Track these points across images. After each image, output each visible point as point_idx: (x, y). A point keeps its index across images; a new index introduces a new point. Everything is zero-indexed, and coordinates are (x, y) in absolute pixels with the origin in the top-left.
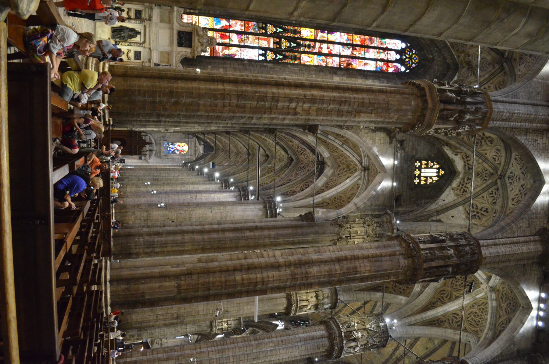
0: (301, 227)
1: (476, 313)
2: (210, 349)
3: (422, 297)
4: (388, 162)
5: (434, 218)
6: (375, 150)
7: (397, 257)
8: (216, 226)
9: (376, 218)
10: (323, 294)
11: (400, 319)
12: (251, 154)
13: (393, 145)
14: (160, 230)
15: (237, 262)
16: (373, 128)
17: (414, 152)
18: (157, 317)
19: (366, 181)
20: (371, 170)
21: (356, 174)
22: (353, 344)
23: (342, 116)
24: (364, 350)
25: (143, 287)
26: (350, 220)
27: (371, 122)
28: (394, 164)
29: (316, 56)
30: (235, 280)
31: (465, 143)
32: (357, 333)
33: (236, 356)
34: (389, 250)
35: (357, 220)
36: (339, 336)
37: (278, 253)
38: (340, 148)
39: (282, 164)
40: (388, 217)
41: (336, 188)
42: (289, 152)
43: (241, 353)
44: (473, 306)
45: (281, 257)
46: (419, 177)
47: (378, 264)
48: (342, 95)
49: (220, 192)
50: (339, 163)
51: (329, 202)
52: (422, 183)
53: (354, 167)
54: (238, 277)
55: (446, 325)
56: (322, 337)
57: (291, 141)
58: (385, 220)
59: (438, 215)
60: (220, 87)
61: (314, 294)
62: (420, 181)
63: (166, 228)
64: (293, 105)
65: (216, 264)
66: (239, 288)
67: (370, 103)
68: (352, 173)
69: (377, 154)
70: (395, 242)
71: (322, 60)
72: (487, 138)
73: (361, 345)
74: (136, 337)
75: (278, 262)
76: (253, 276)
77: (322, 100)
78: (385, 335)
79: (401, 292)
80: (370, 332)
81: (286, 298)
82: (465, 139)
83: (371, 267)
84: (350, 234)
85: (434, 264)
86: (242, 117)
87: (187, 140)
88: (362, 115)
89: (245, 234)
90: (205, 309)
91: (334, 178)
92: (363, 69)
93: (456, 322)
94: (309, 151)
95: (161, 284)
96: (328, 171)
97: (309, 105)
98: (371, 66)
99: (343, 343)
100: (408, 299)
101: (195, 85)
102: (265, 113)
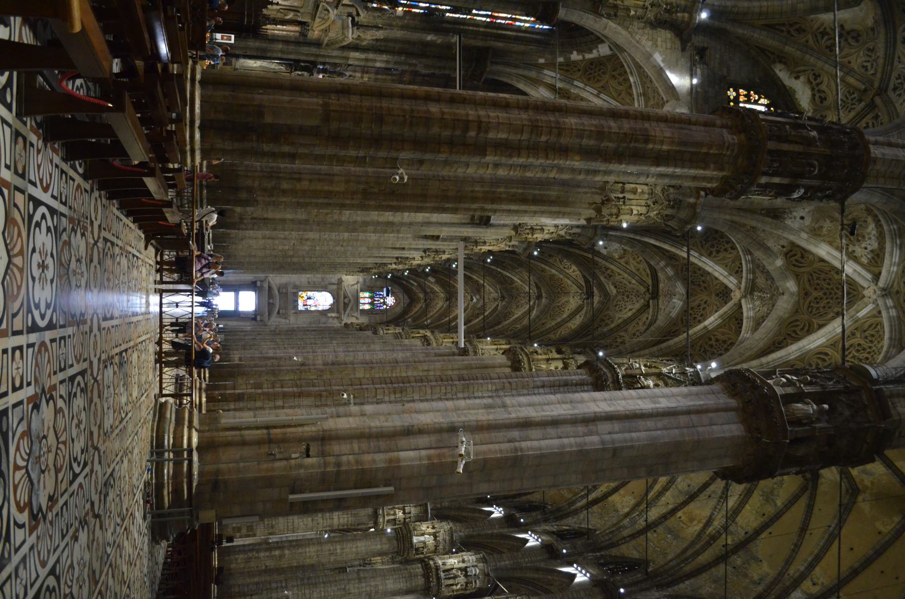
1: (859, 345)
4: (679, 80)
6: (658, 58)
17: (725, 70)
28: (692, 85)
31: (812, 49)
36: (613, 382)
44: (853, 334)
66: (435, 130)
69: (662, 65)
72: (848, 33)
74: (244, 531)
81: (511, 367)
82: (811, 42)
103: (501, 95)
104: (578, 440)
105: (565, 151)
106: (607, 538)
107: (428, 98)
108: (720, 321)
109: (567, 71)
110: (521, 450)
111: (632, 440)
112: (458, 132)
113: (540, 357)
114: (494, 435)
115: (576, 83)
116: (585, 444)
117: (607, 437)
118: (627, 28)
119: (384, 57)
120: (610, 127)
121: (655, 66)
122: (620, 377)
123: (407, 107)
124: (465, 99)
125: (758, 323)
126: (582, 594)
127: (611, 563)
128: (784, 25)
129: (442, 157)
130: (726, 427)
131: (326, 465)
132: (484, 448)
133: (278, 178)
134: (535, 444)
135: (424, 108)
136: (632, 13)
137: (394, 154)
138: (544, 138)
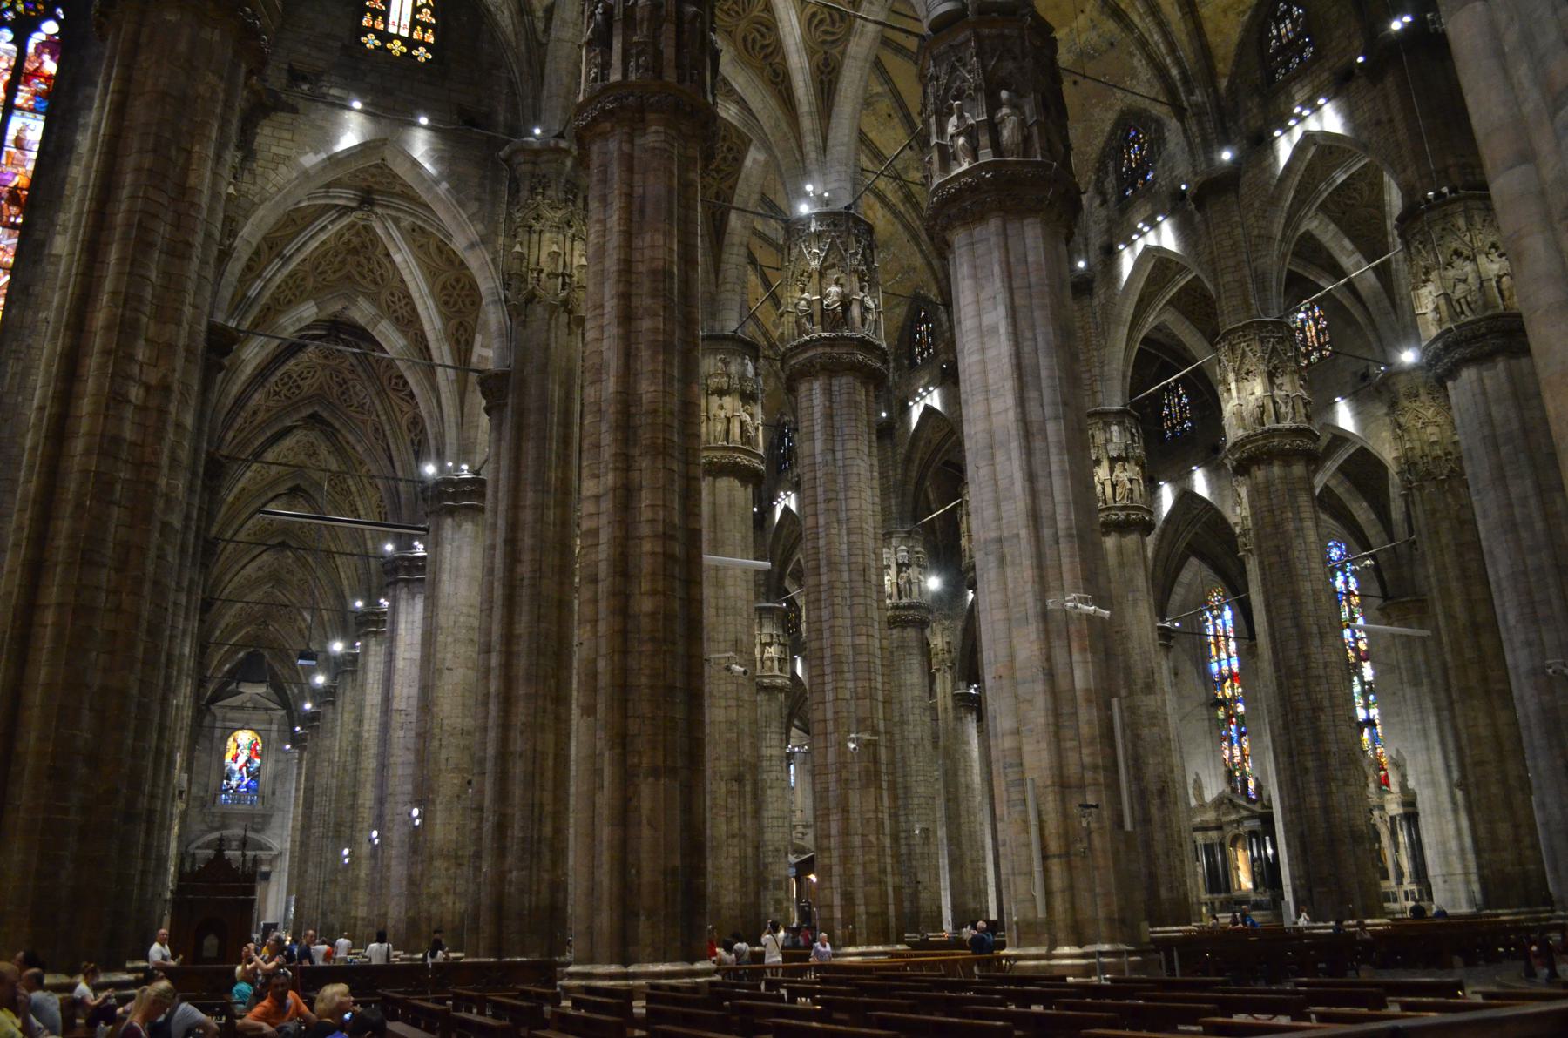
0: (520, 413)
2: (829, 696)
3: (755, 102)
4: (351, 132)
5: (540, 26)
6: (310, 160)
7: (637, 153)
8: (495, 660)
9: (518, 191)
10: (715, 375)
11: (805, 174)
12: (283, 540)
13: (302, 105)
14: (490, 819)
15: (602, 605)
16: (239, 155)
18: (734, 836)
19: (405, 204)
20: (372, 181)
21: (380, 232)
22: (856, 311)
23: (189, 245)
24: (873, 285)
25: (648, 871)
26: (515, 267)
27: (218, 157)
30: (653, 615)
32: (828, 295)
33: (852, 626)
34: (616, 172)
35: (518, 248)
36: (832, 346)
37: (589, 487)
38: (293, 265)
39: (323, 449)
40: (521, 158)
41: (415, 295)
42: (288, 423)
43: (847, 612)
45: (603, 480)
46: (410, 43)
47: (649, 210)
48: (118, 234)
49: (392, 640)
50: (338, 275)
51: (454, 322)
52: (432, 40)
53: (358, 234)
54: (646, 605)
55: (835, 51)
56: (828, 392)
57: (255, 413)
58: (526, 168)
59: (531, 13)
60: (49, 617)
61: (715, 400)
62: (423, 43)
63: (487, 803)
64: (135, 393)
65: (602, 664)
66: (677, 605)
67: (154, 151)
68: (375, 241)
69: (323, 156)
70: (595, 148)
73: (862, 289)
74: (781, 894)
75: (614, 489)
76: (646, 565)
77: (128, 300)
78: (843, 223)
79: (735, 159)
80: (830, 261)
81: (715, 478)
83: (657, 230)
84: (556, 276)
85: (669, 52)
86: (161, 557)
87: (218, 733)
88: (192, 181)
89: (527, 575)
90: (723, 703)
91: (385, 295)
92: (33, 156)
93: (833, 23)
94: (293, 361)
95: (645, 822)
96: (362, 312)
97: (141, 343)
99: (851, 339)
100: (755, 141)
101: (35, 698)
102: (152, 484)
104: (1053, 450)
110: (1069, 528)
111: (1052, 377)
114: (1050, 561)
116: (1060, 442)
117: (1048, 411)
118: (254, 206)
121: (324, 169)
123: (647, 647)
127: (911, 350)
130: (1030, 242)
131: (1096, 784)
132: (1067, 576)
133: (539, 841)
134: (1060, 509)
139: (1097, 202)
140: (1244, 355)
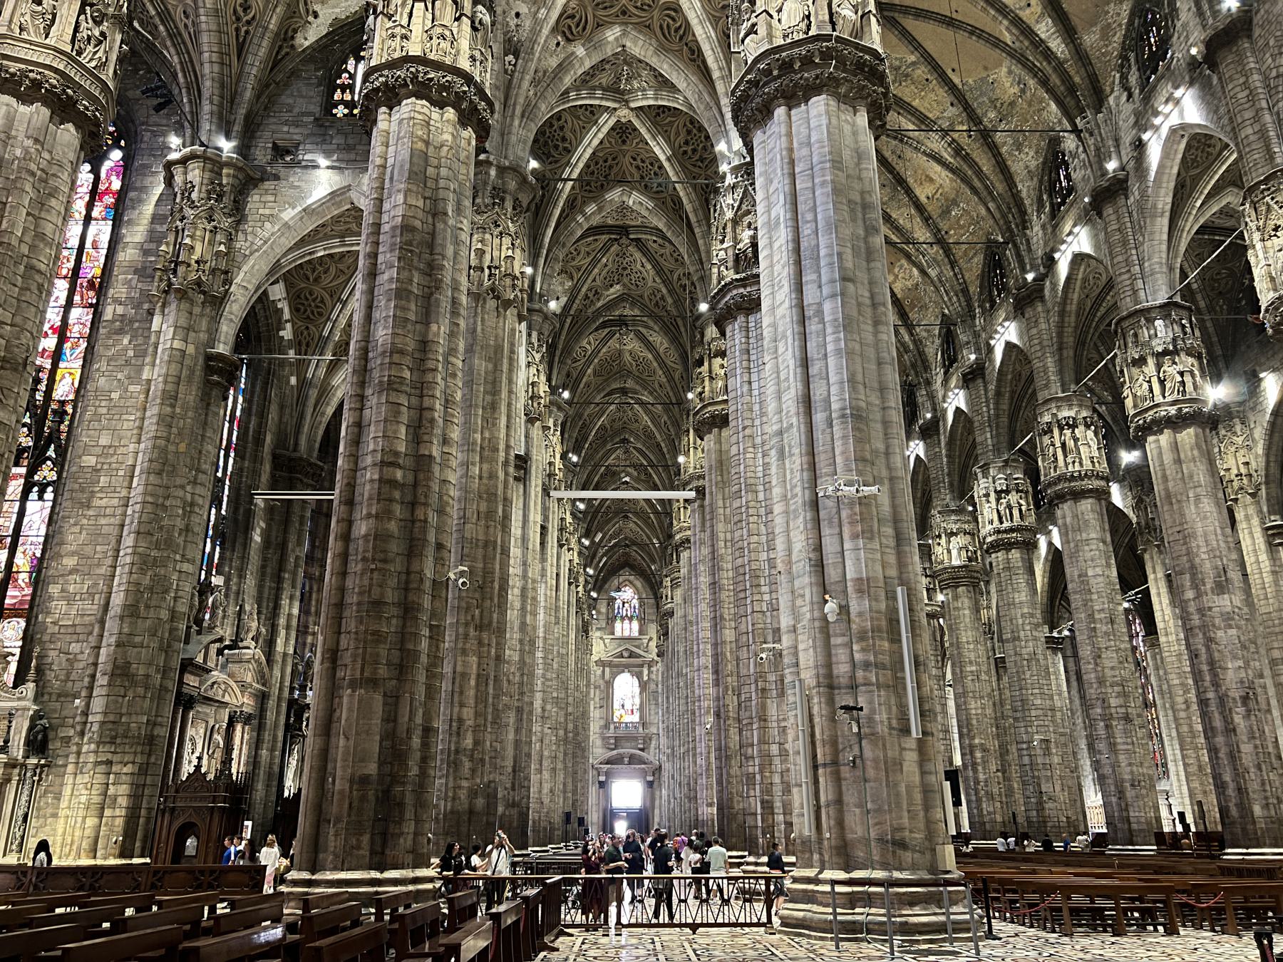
6: (288, 214)
17: (305, 119)
29: (62, 365)
36: (745, 286)
66: (393, 526)
69: (300, 209)
71: (72, 348)
81: (721, 428)
92: (104, 252)
98: (101, 231)
103: (343, 433)
105: (425, 345)
106: (955, 299)
107: (346, 537)
108: (660, 139)
109: (308, 345)
112: (397, 495)
113: (707, 389)
114: (820, 448)
115: (326, 333)
119: (285, 602)
120: (391, 280)
122: (738, 277)
124: (348, 484)
125: (664, 84)
126: (1034, 331)
127: (990, 292)
128: (237, 30)
129: (433, 518)
133: (457, 752)
134: (834, 390)
135: (361, 542)
136: (222, 248)
137: (427, 585)
138: (407, 374)
139: (1124, 98)
140: (1269, 209)
